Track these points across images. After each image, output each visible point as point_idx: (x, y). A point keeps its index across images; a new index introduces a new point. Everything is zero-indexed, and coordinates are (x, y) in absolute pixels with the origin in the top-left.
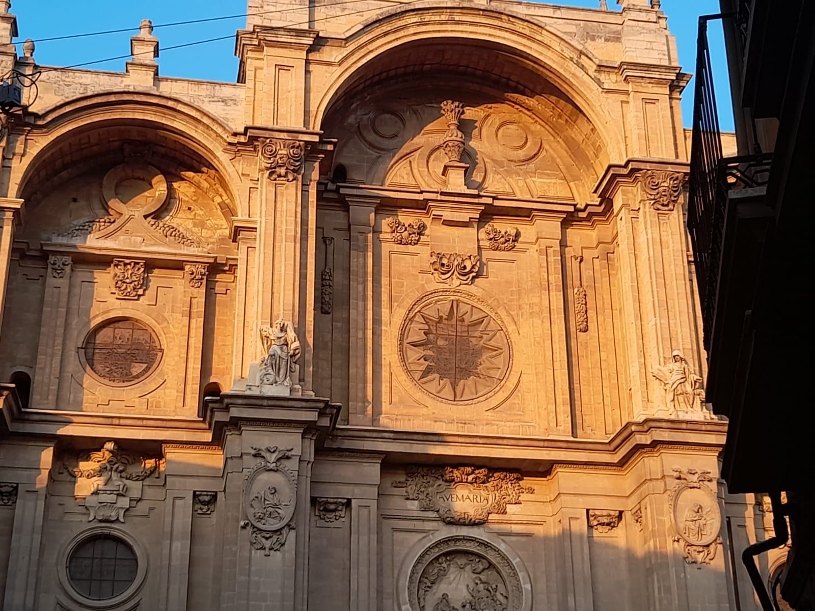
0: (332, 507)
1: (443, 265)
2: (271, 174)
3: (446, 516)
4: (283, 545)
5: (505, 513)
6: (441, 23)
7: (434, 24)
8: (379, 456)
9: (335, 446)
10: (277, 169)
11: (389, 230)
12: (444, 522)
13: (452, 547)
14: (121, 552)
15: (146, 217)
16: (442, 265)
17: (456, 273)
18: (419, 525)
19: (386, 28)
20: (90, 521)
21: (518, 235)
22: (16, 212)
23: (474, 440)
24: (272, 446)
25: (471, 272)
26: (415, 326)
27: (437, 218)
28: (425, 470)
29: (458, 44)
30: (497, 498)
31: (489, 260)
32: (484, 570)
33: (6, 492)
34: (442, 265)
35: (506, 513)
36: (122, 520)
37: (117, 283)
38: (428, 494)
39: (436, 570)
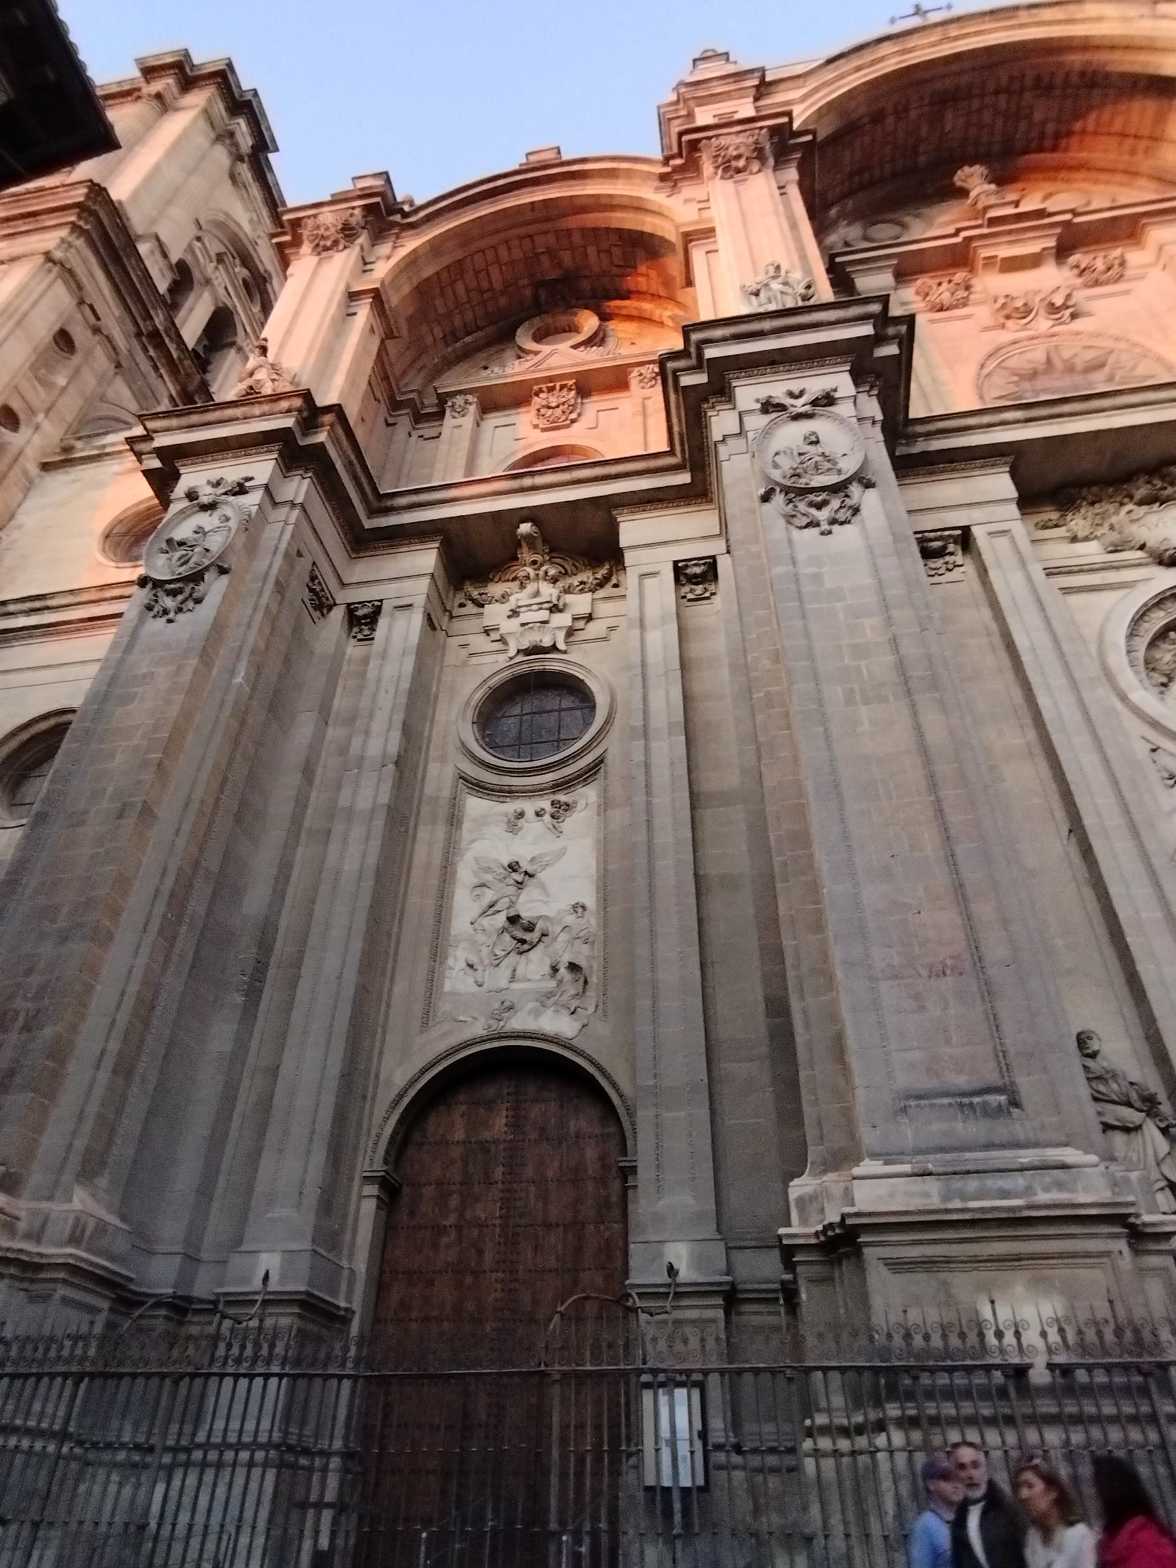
1: (1017, 309)
2: (726, 170)
3: (1163, 548)
4: (856, 510)
6: (933, 45)
7: (923, 48)
8: (1004, 459)
10: (734, 164)
11: (919, 298)
14: (567, 702)
15: (575, 347)
19: (855, 62)
20: (511, 658)
22: (377, 296)
24: (795, 386)
25: (1065, 306)
26: (997, 379)
27: (990, 261)
28: (1095, 489)
29: (962, 72)
33: (365, 617)
36: (561, 646)
37: (538, 410)
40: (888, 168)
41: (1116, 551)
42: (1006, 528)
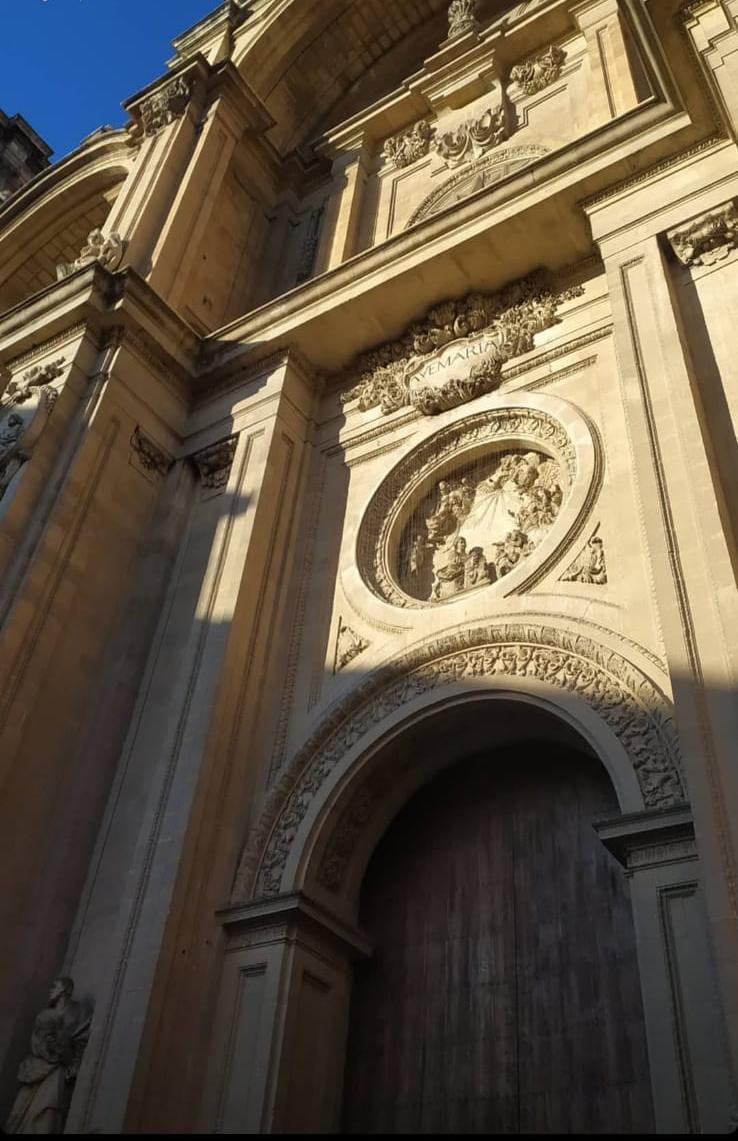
0: (212, 459)
5: (528, 347)
9: (209, 369)
12: (426, 415)
13: (452, 453)
16: (455, 146)
17: (474, 142)
18: (386, 440)
21: (560, 58)
23: (409, 242)
30: (513, 332)
31: (526, 110)
32: (534, 473)
34: (455, 146)
35: (533, 347)
38: (392, 386)
39: (442, 509)
40: (404, 26)
41: (390, 412)
42: (261, 427)
